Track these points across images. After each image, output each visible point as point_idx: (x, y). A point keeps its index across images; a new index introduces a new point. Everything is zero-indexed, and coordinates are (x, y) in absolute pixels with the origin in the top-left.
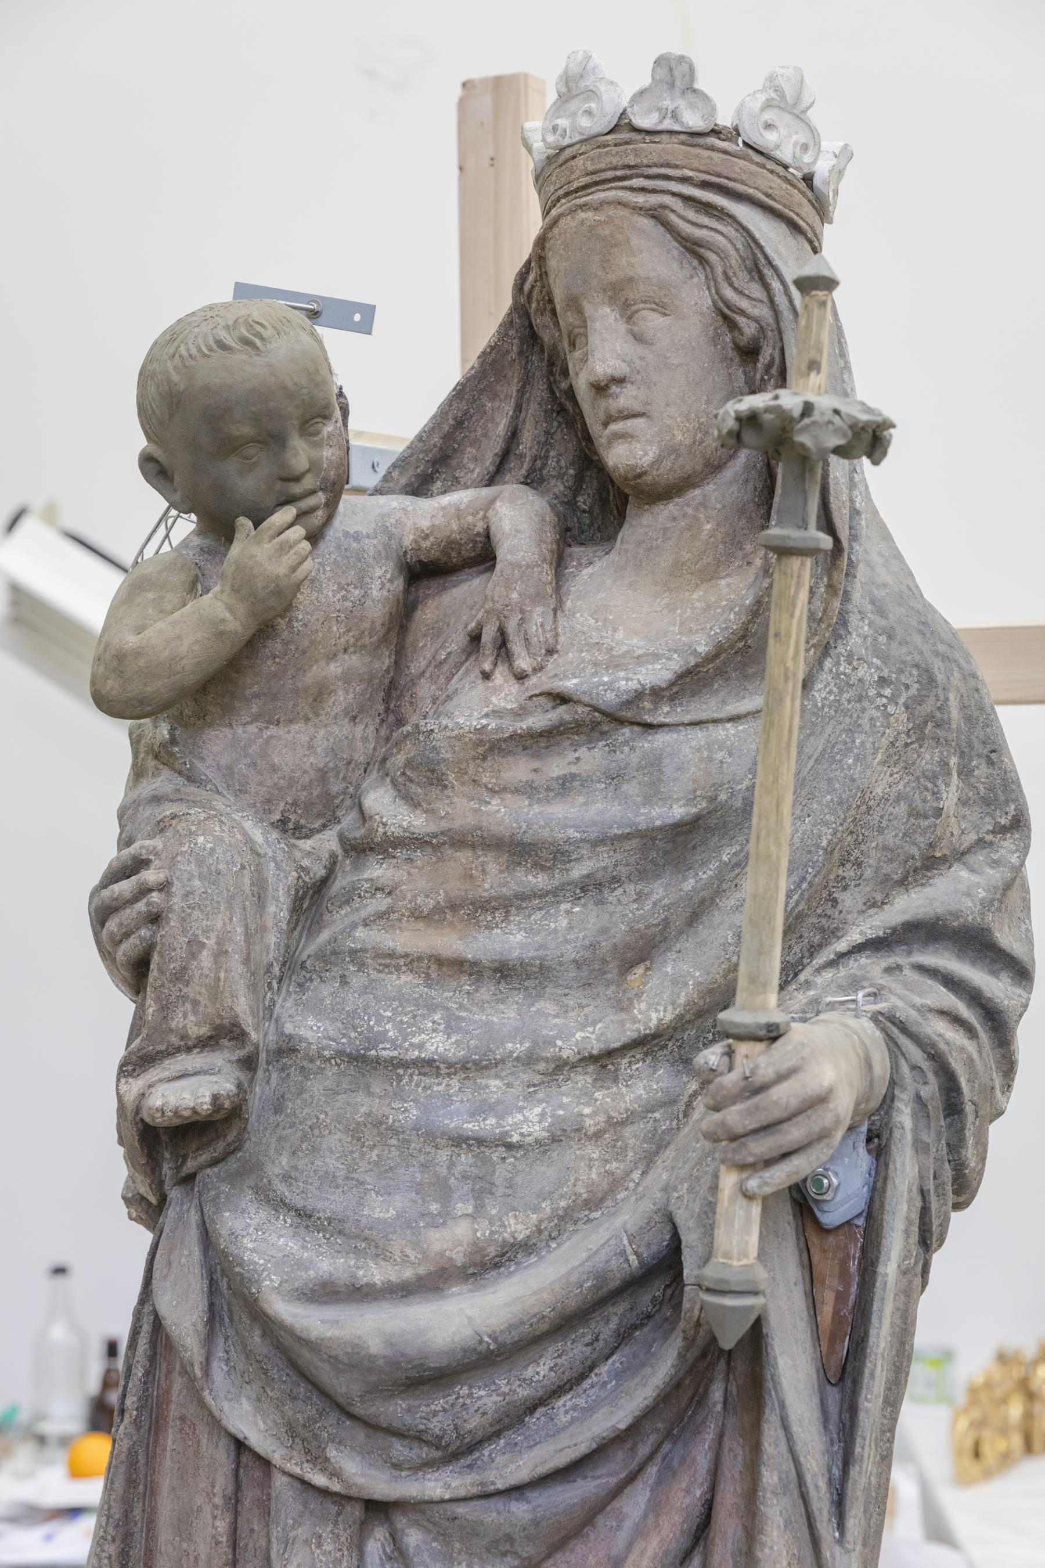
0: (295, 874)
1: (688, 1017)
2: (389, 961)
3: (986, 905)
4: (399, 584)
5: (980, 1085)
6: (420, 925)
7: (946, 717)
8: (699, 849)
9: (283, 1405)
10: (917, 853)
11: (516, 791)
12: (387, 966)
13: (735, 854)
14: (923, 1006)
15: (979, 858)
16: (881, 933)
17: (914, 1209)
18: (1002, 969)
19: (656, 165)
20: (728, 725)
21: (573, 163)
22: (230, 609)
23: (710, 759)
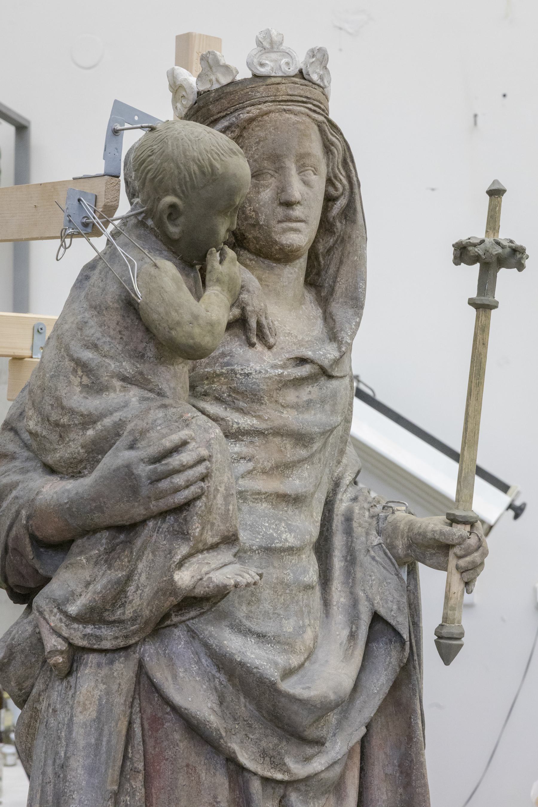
2: (258, 496)
6: (265, 477)
9: (261, 741)
11: (292, 407)
12: (256, 499)
21: (278, 86)
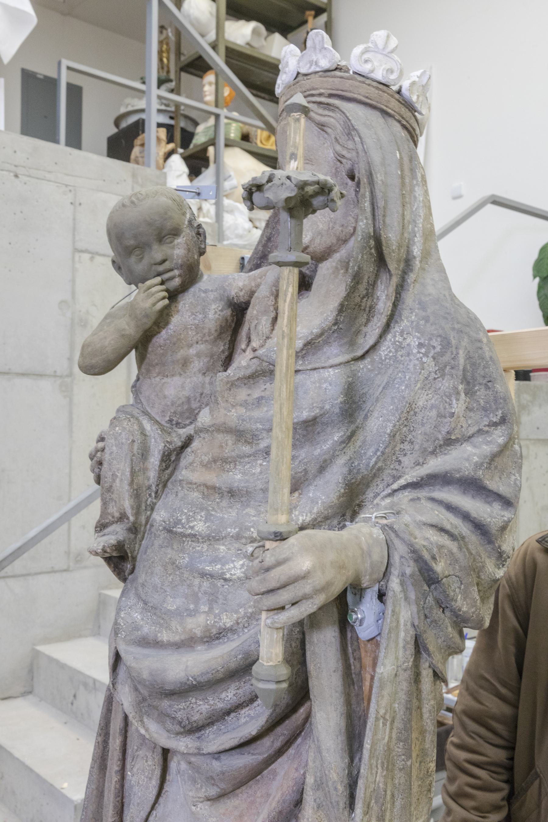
0: (163, 445)
1: (319, 519)
2: (190, 486)
3: (478, 466)
4: (228, 312)
5: (460, 567)
6: (204, 469)
7: (456, 363)
8: (322, 434)
10: (440, 437)
11: (241, 405)
13: (341, 437)
14: (420, 521)
15: (479, 439)
16: (415, 480)
17: (409, 635)
18: (494, 501)
19: (308, 90)
20: (330, 370)
22: (128, 324)
23: (320, 387)
